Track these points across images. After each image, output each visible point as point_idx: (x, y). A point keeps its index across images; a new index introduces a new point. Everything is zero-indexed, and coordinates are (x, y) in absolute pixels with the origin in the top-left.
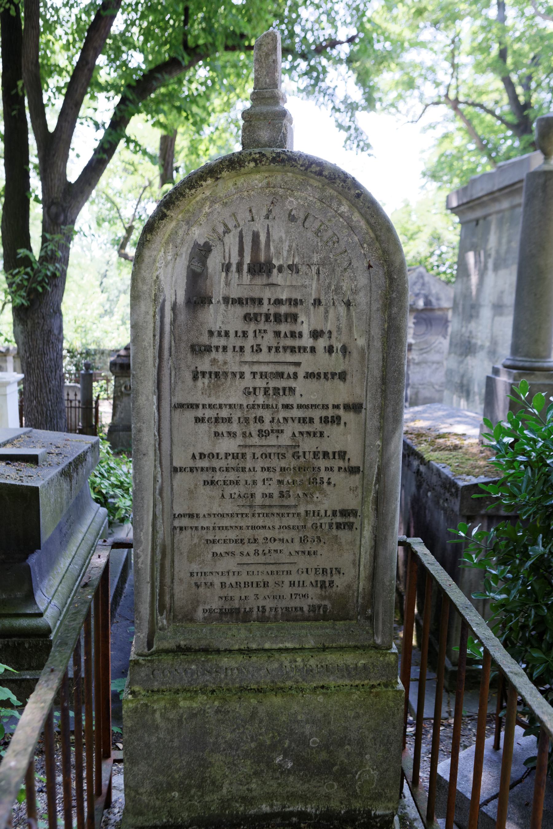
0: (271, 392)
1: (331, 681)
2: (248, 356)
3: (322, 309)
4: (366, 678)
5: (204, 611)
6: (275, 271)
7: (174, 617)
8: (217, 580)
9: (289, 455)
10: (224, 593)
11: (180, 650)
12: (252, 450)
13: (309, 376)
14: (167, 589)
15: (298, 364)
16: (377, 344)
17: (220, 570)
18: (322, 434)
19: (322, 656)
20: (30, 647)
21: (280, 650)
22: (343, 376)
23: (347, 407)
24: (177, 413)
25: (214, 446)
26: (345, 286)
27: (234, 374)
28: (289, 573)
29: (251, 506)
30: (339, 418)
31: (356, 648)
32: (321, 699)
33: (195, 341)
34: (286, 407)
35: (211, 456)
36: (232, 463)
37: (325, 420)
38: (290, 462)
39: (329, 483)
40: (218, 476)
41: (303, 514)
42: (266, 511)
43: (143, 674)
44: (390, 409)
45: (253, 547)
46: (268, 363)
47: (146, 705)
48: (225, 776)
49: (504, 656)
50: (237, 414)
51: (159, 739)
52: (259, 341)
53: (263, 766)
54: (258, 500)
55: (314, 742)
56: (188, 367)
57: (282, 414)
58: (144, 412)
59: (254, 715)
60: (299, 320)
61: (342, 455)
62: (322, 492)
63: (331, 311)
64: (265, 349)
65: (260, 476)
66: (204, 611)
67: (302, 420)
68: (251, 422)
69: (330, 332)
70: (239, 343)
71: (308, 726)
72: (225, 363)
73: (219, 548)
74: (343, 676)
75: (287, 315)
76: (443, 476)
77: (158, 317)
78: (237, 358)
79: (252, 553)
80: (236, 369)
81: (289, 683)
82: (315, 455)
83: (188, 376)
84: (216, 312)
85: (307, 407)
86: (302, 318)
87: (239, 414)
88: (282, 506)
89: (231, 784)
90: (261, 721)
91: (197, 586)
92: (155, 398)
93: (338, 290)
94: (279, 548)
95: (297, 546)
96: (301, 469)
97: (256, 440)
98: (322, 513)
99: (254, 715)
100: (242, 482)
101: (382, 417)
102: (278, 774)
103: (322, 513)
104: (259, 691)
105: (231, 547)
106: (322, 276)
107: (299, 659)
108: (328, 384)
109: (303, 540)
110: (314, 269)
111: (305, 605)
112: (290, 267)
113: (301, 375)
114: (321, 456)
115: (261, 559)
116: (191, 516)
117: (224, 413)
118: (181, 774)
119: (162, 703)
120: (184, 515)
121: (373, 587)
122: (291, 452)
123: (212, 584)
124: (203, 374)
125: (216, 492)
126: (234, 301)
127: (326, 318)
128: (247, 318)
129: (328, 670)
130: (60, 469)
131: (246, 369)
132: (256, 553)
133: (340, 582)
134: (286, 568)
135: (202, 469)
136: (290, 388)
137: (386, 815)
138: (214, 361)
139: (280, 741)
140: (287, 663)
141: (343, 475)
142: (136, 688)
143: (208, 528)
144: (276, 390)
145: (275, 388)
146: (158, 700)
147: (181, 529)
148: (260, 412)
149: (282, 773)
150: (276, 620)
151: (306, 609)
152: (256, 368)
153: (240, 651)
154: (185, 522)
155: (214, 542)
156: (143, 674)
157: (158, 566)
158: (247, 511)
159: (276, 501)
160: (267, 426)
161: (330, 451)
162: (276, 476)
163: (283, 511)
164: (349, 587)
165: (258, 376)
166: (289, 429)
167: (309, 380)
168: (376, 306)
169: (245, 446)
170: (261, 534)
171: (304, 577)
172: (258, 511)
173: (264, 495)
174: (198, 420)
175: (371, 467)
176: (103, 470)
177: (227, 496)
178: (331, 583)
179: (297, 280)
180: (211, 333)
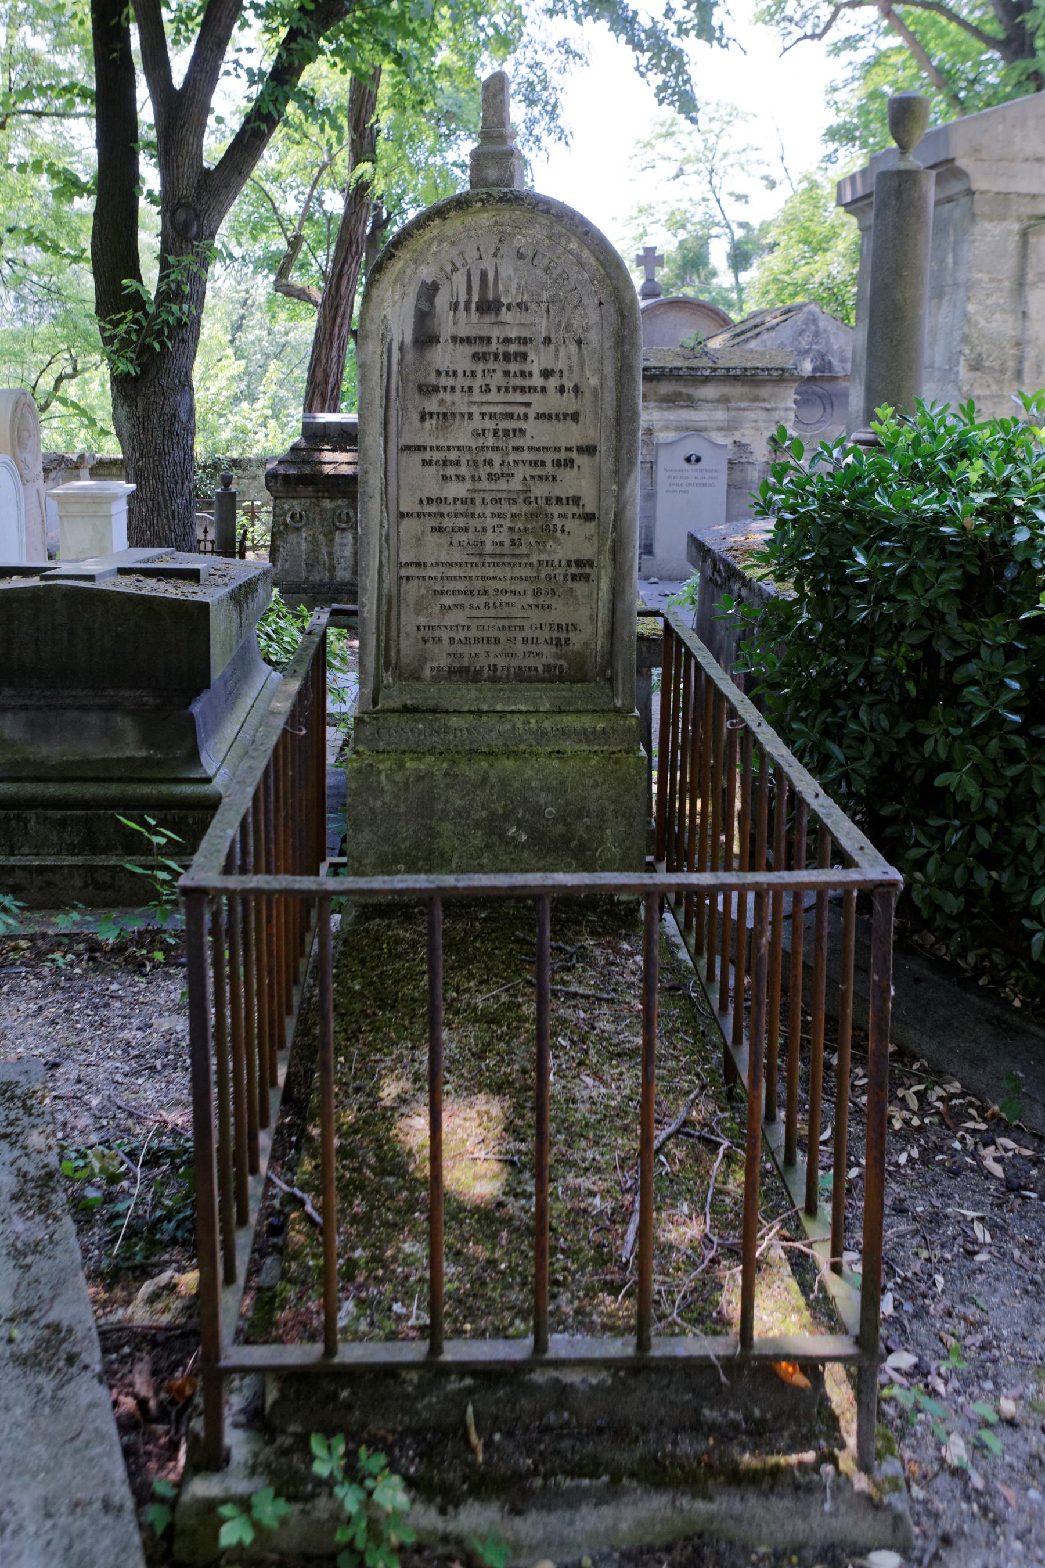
0: (500, 433)
1: (568, 746)
2: (477, 397)
3: (552, 347)
4: (605, 744)
5: (432, 669)
6: (504, 309)
7: (399, 676)
8: (445, 636)
9: (520, 500)
10: (452, 649)
11: (406, 709)
12: (482, 495)
13: (540, 416)
14: (393, 644)
15: (528, 405)
16: (611, 383)
17: (448, 624)
18: (554, 478)
19: (558, 718)
20: (194, 823)
21: (513, 712)
22: (575, 417)
23: (581, 450)
24: (404, 456)
25: (442, 489)
26: (576, 323)
27: (462, 415)
28: (522, 628)
29: (480, 555)
30: (572, 461)
31: (595, 711)
32: (556, 763)
33: (422, 381)
34: (517, 449)
35: (439, 501)
36: (460, 508)
37: (557, 463)
38: (522, 508)
39: (563, 531)
40: (447, 523)
41: (536, 564)
42: (497, 560)
43: (367, 733)
44: (624, 451)
45: (484, 599)
46: (497, 403)
47: (371, 765)
48: (454, 848)
49: (829, 815)
50: (466, 457)
51: (384, 803)
52: (488, 380)
53: (495, 838)
54: (489, 548)
55: (550, 813)
56: (416, 408)
57: (512, 457)
58: (370, 453)
59: (484, 780)
60: (529, 359)
61: (576, 500)
62: (556, 539)
63: (562, 349)
64: (494, 389)
65: (490, 522)
66: (432, 669)
67: (534, 464)
68: (481, 465)
69: (561, 371)
70: (467, 383)
71: (543, 795)
72: (453, 404)
73: (447, 600)
74: (580, 741)
75: (516, 354)
76: (765, 596)
77: (385, 357)
78: (466, 399)
79: (482, 606)
80: (464, 409)
81: (522, 747)
82: (548, 500)
83: (415, 417)
84: (444, 351)
85: (538, 449)
86: (532, 356)
87: (468, 457)
88: (513, 555)
89: (460, 857)
90: (493, 787)
91: (425, 641)
92: (382, 439)
93: (568, 327)
94: (511, 601)
95: (531, 600)
96: (533, 516)
97: (485, 484)
98: (556, 563)
99: (484, 780)
100: (471, 529)
101: (617, 459)
102: (511, 849)
103: (556, 563)
104: (490, 753)
105: (460, 599)
106: (552, 314)
107: (532, 721)
108: (560, 426)
109: (536, 593)
110: (544, 306)
111: (539, 664)
112: (519, 305)
113: (532, 415)
114: (554, 501)
115: (492, 613)
116: (418, 565)
117: (453, 456)
118: (408, 844)
119: (388, 764)
120: (411, 564)
121: (612, 645)
122: (522, 496)
123: (440, 640)
124: (431, 414)
125: (444, 539)
126: (462, 340)
127: (557, 356)
128: (475, 357)
129: (564, 733)
130: (229, 589)
131: (475, 410)
132: (487, 605)
133: (577, 640)
134: (518, 623)
135: (430, 515)
136: (521, 430)
137: (630, 902)
138: (442, 402)
139: (513, 810)
140: (520, 725)
141: (577, 522)
142: (361, 748)
143: (436, 578)
144: (506, 431)
145: (504, 430)
146: (383, 760)
147: (408, 578)
148: (489, 455)
149: (515, 847)
150: (508, 680)
151: (540, 669)
152: (485, 409)
153: (470, 712)
154: (412, 571)
155: (442, 593)
156: (367, 733)
157: (383, 617)
158: (476, 560)
159: (507, 549)
160: (497, 469)
161: (563, 496)
162: (507, 523)
163: (514, 560)
164: (586, 645)
165: (487, 417)
166: (520, 472)
167: (540, 421)
168: (608, 344)
169: (475, 491)
170: (491, 585)
171: (538, 633)
172: (489, 560)
173: (495, 543)
174: (426, 463)
175: (607, 514)
176: (269, 630)
177: (455, 543)
178: (568, 640)
179: (527, 318)
180: (439, 373)
